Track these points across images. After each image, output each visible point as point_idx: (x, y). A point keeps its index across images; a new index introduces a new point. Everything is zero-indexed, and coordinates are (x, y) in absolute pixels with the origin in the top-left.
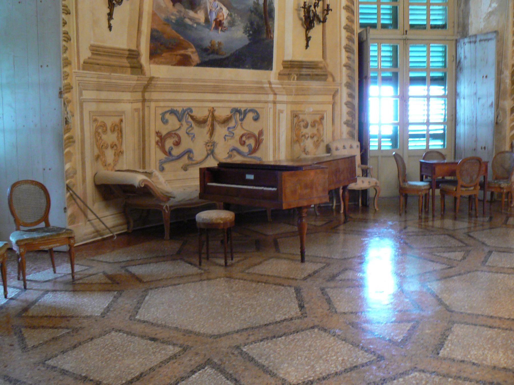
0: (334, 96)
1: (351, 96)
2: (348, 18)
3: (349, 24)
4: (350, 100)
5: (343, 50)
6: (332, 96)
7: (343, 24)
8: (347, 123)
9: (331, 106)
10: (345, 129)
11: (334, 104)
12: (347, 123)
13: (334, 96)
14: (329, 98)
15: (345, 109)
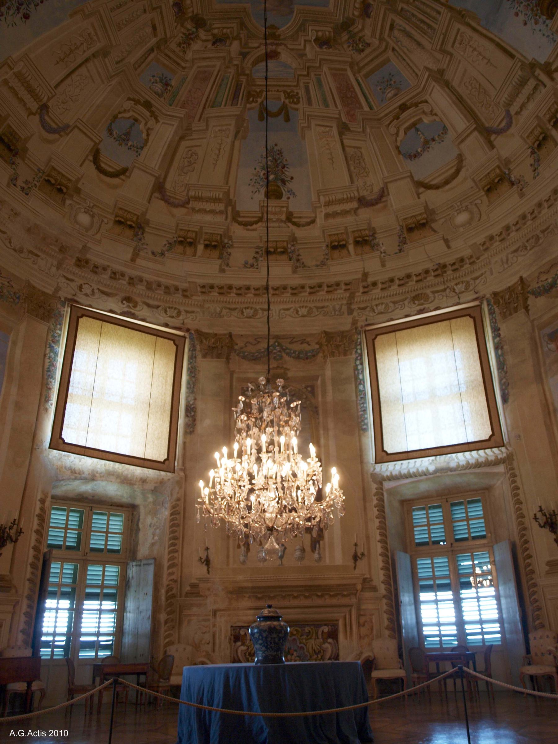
0: (14, 606)
1: (30, 606)
2: (37, 540)
3: (37, 545)
4: (28, 610)
5: (29, 566)
6: (12, 606)
7: (32, 545)
8: (23, 632)
9: (10, 615)
10: (21, 637)
11: (13, 614)
12: (23, 632)
13: (14, 606)
14: (10, 608)
15: (23, 619)
